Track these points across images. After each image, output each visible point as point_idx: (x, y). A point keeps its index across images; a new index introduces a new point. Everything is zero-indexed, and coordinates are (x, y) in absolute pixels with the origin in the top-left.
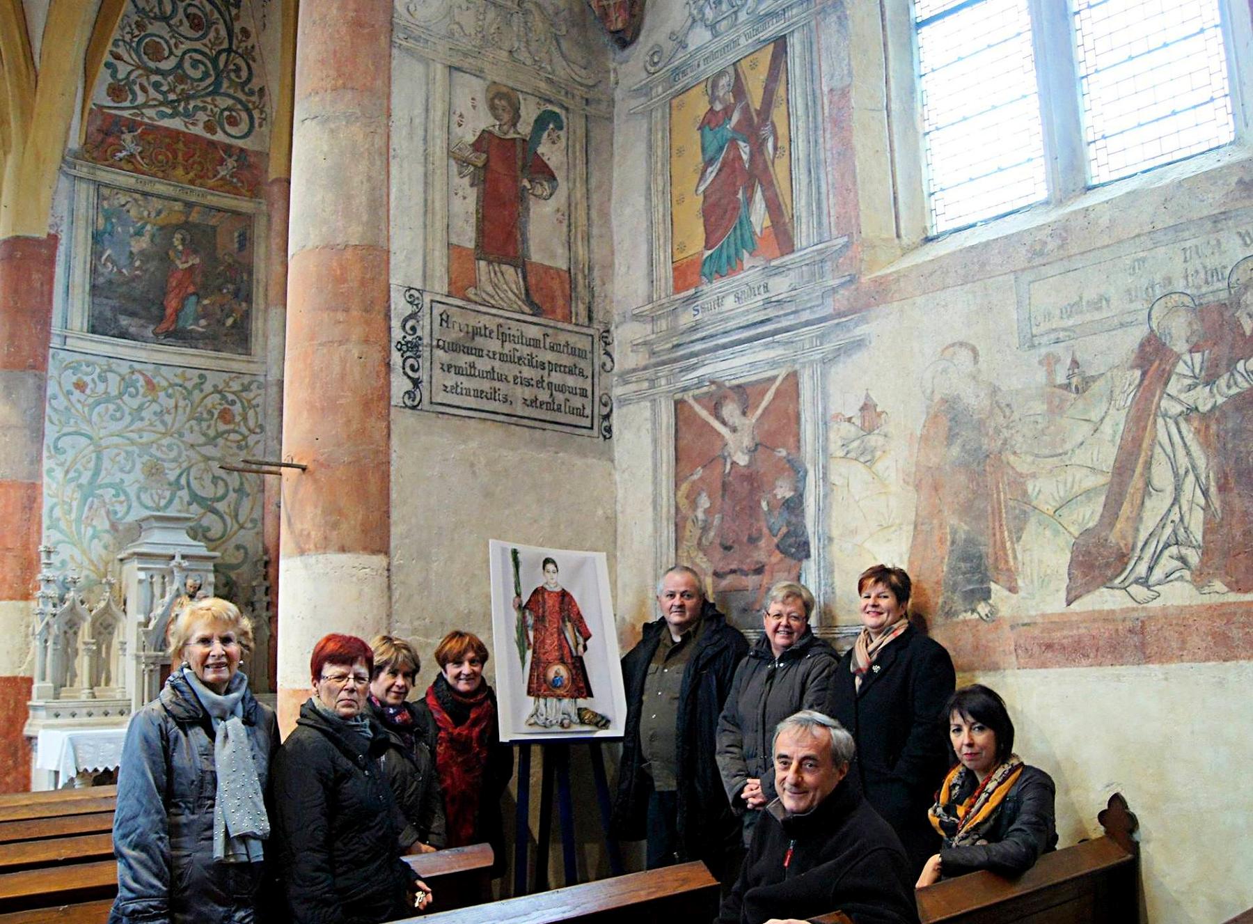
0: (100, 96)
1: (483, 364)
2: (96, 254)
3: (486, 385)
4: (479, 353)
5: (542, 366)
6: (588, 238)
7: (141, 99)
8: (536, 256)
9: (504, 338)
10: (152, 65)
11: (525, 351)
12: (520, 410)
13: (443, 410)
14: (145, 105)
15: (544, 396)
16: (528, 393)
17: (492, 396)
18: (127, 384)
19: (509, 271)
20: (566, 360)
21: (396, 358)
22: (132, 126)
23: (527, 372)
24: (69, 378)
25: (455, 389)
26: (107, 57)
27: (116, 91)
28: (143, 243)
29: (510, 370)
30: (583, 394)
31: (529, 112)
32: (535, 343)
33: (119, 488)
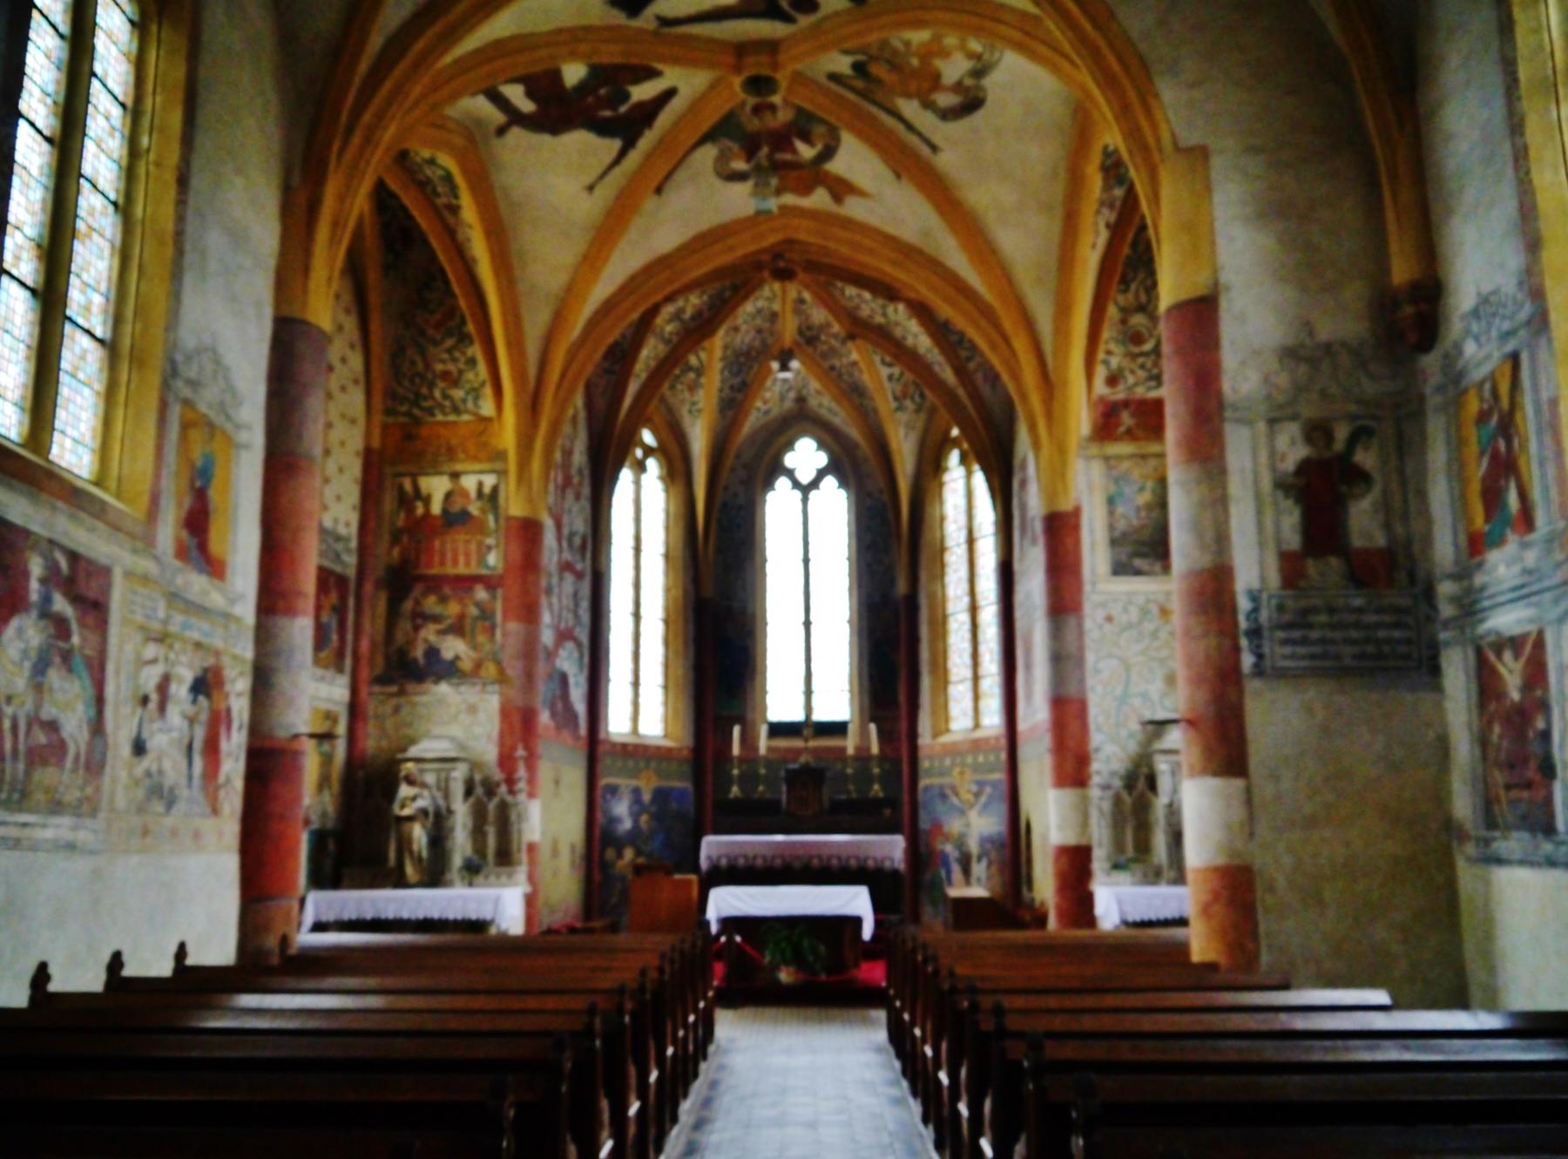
0: (1100, 388)
1: (1315, 634)
2: (1111, 513)
3: (1317, 650)
4: (1310, 626)
5: (1368, 627)
6: (1405, 517)
7: (1131, 380)
8: (1357, 542)
9: (1332, 610)
10: (1136, 350)
11: (1351, 618)
12: (1348, 662)
13: (1281, 674)
14: (1136, 384)
15: (1370, 649)
16: (1356, 650)
17: (1324, 656)
18: (1144, 612)
19: (1334, 562)
20: (1387, 618)
21: (1244, 642)
22: (1126, 404)
23: (1354, 634)
24: (1100, 614)
25: (1292, 657)
26: (1101, 355)
27: (1112, 380)
28: (1146, 497)
29: (1337, 635)
30: (1409, 642)
31: (1342, 433)
32: (1360, 610)
33: (1145, 696)
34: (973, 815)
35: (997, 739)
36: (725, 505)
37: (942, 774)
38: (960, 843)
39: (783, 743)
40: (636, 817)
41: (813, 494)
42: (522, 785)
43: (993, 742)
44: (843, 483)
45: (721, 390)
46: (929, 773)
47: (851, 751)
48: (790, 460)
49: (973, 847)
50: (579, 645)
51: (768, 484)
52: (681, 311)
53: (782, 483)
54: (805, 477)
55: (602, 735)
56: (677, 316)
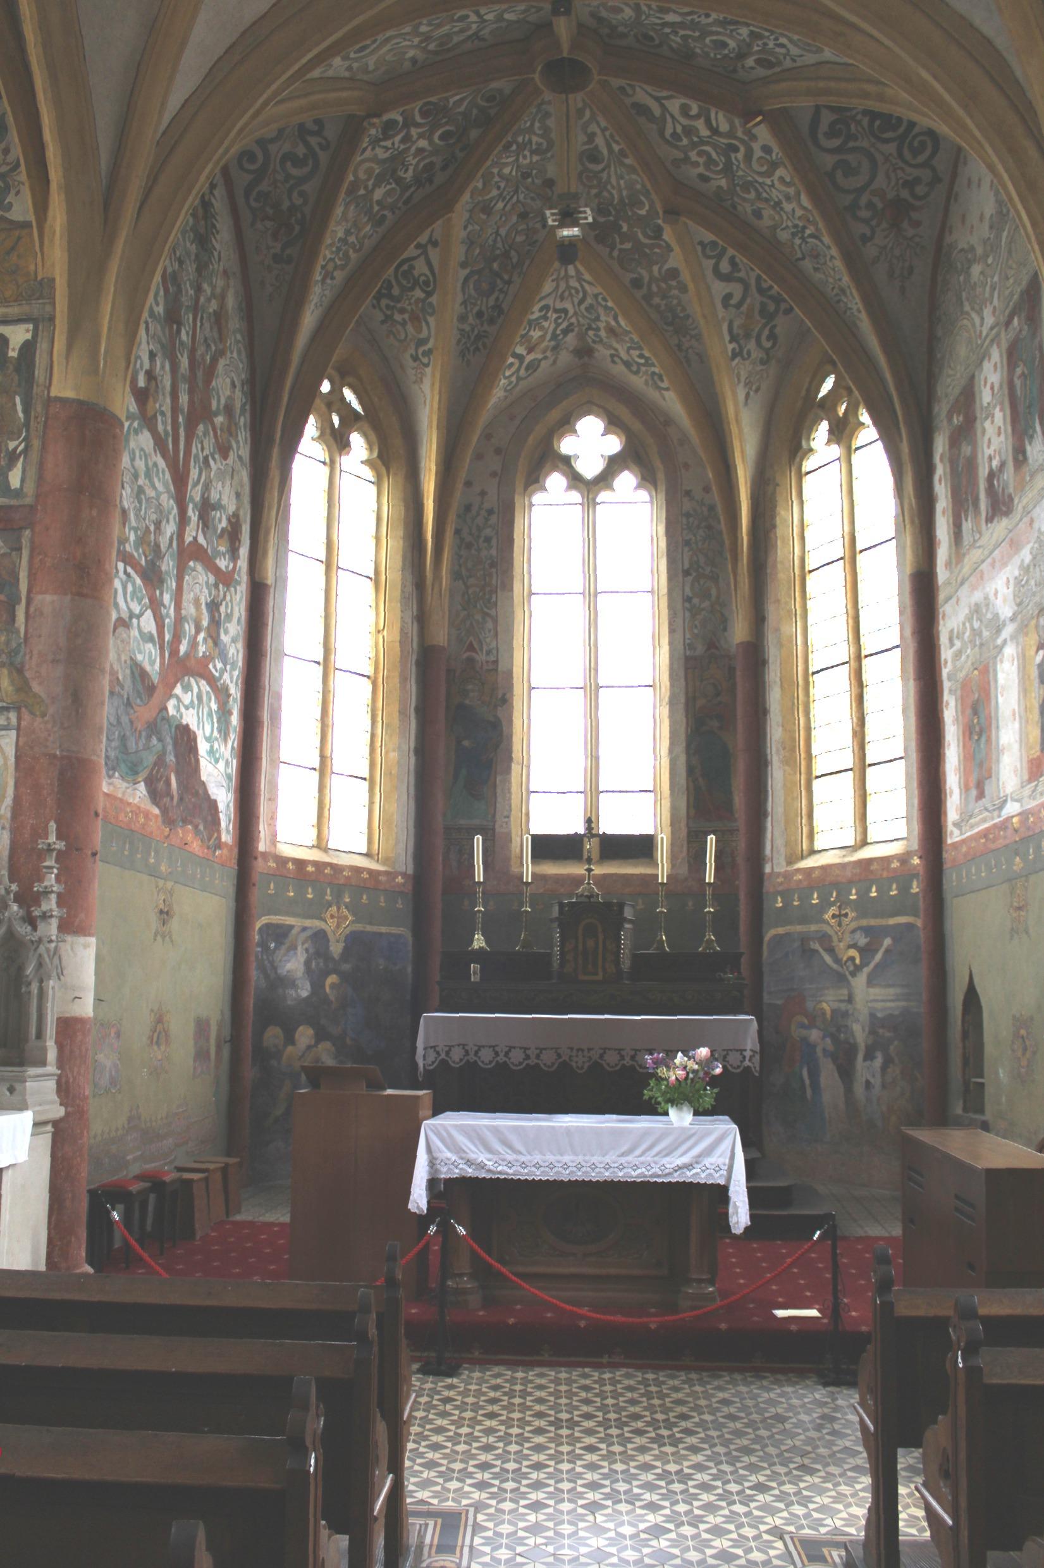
34: (859, 982)
35: (904, 858)
36: (468, 508)
37: (804, 920)
38: (837, 1024)
39: (551, 869)
40: (317, 980)
41: (603, 496)
42: (51, 904)
43: (895, 864)
44: (648, 479)
45: (463, 318)
46: (784, 916)
47: (663, 878)
48: (567, 445)
49: (859, 1034)
50: (222, 693)
51: (534, 480)
52: (397, 159)
53: (556, 481)
54: (590, 467)
55: (262, 847)
56: (392, 166)
